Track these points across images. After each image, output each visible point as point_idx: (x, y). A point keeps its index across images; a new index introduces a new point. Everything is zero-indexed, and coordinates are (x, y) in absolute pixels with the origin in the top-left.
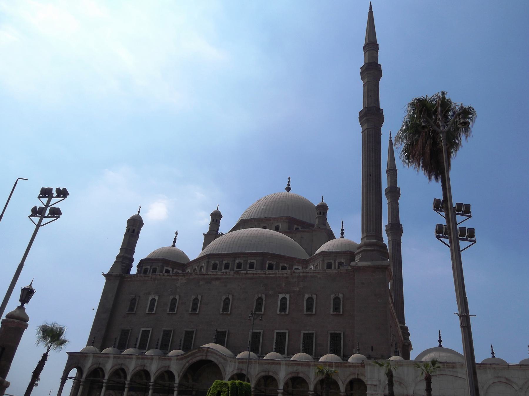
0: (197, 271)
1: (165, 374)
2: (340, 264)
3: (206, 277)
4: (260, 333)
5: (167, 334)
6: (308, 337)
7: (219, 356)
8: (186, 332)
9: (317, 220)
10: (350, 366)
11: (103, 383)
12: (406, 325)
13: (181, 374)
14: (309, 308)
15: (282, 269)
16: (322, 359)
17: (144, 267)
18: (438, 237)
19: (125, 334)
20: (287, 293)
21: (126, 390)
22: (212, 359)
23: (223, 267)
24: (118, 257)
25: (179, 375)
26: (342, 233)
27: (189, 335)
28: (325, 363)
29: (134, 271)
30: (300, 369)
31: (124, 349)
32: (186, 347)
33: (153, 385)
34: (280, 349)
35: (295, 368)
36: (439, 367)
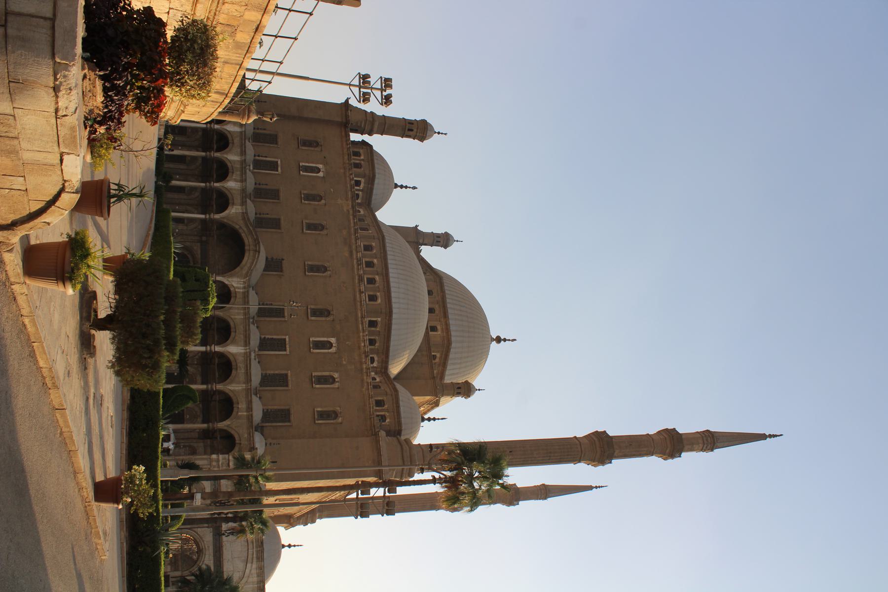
2: (383, 418)
4: (284, 317)
5: (274, 194)
8: (279, 219)
10: (249, 434)
12: (318, 520)
15: (370, 340)
17: (361, 151)
19: (272, 139)
20: (338, 348)
21: (203, 154)
23: (367, 260)
26: (429, 419)
27: (275, 224)
29: (355, 137)
30: (241, 371)
33: (210, 187)
34: (265, 344)
35: (241, 366)
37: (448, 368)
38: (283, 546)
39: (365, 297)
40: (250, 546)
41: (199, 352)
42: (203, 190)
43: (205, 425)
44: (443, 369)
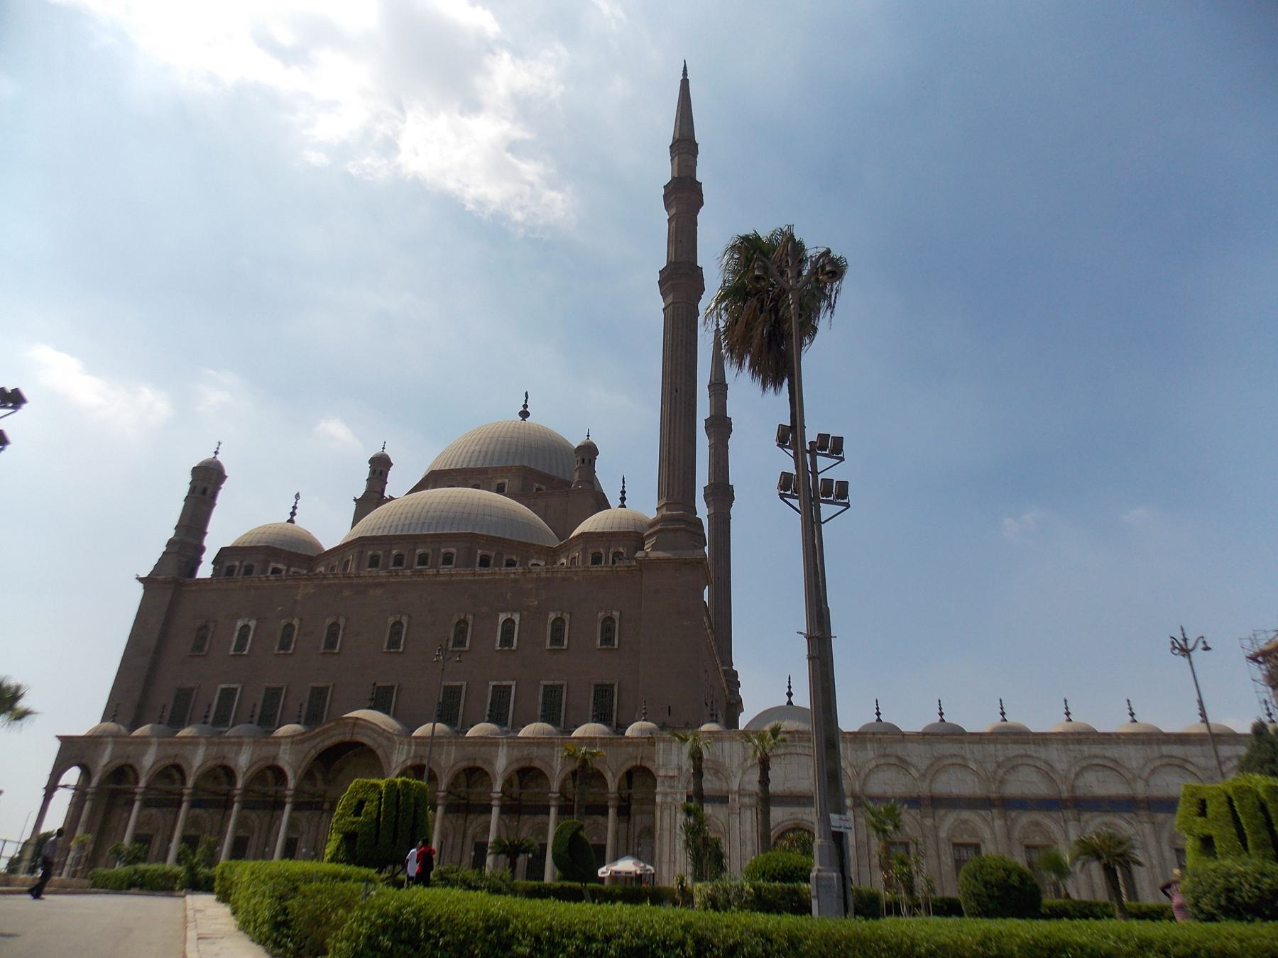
0: (338, 570)
1: (269, 773)
2: (617, 555)
3: (355, 581)
5: (272, 695)
6: (553, 694)
7: (379, 734)
8: (313, 688)
9: (577, 474)
10: (628, 744)
11: (135, 794)
13: (300, 771)
14: (557, 638)
16: (577, 733)
17: (227, 564)
18: (782, 496)
20: (514, 611)
22: (365, 740)
24: (171, 543)
25: (295, 773)
26: (623, 499)
27: (319, 695)
28: (581, 740)
29: (205, 570)
31: (182, 726)
32: (312, 718)
34: (497, 716)
36: (784, 740)
37: (554, 473)
38: (790, 703)
39: (444, 570)
40: (793, 750)
41: (499, 818)
42: (245, 805)
43: (611, 811)
44: (554, 475)
